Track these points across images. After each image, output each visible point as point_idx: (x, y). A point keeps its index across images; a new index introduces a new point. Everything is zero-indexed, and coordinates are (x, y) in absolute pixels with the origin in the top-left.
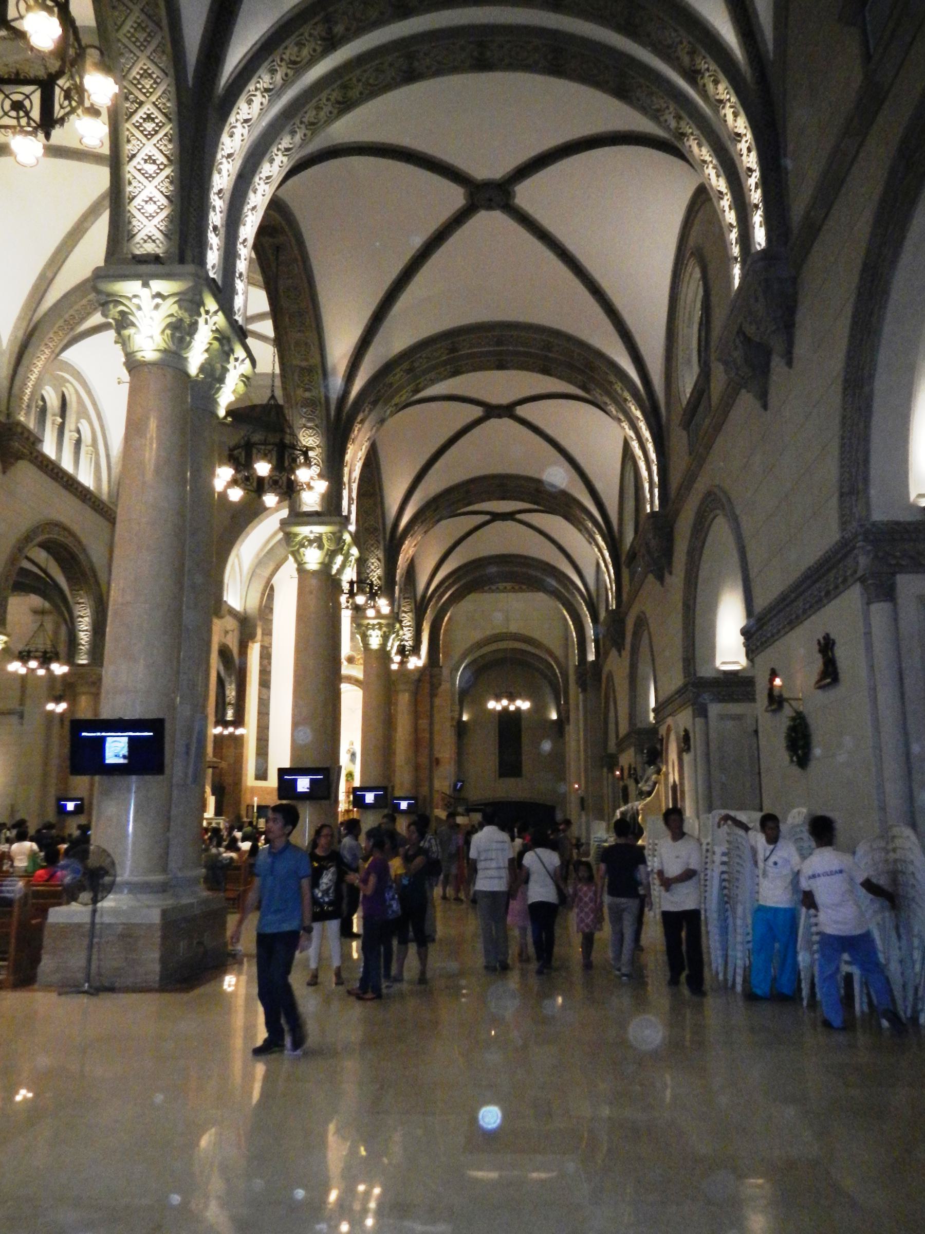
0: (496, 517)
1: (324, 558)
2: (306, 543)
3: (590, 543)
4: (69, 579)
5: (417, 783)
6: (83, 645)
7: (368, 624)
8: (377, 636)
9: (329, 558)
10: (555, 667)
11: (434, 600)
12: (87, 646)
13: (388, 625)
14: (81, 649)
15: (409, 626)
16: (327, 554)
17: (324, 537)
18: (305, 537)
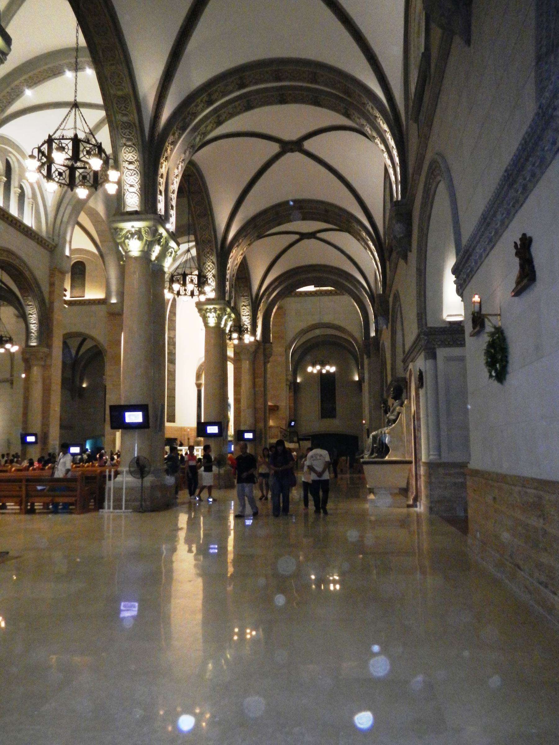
0: (303, 236)
1: (144, 247)
2: (129, 236)
3: (366, 249)
4: (20, 289)
5: (256, 421)
6: (34, 333)
7: (207, 309)
8: (213, 317)
9: (148, 247)
10: (353, 342)
11: (265, 297)
12: (35, 334)
13: (220, 309)
14: (32, 336)
15: (248, 315)
16: (145, 244)
17: (143, 230)
18: (128, 231)
